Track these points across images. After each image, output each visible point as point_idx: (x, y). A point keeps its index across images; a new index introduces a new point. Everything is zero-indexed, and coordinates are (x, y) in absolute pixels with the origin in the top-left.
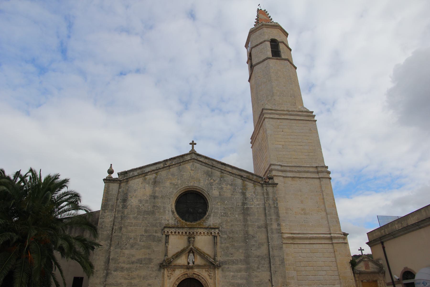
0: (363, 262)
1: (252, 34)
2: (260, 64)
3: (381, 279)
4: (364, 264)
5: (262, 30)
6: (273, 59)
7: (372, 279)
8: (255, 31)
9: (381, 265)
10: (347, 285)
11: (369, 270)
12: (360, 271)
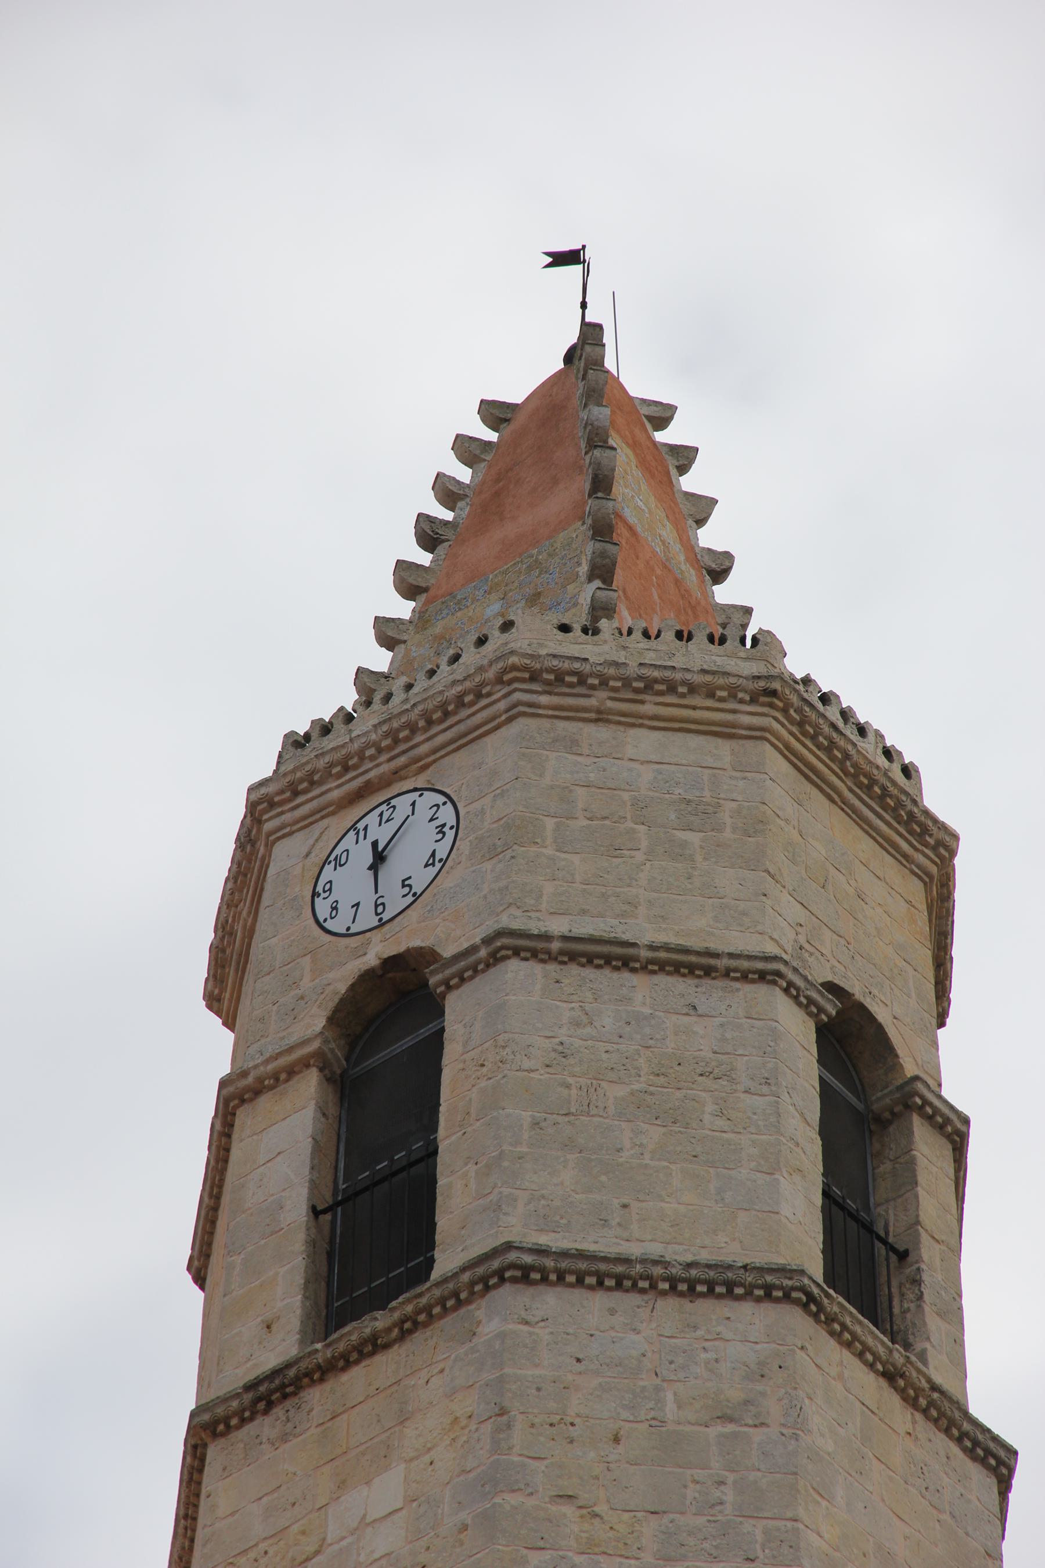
1: (532, 710)
2: (635, 1299)
5: (723, 751)
6: (849, 1345)
8: (599, 699)
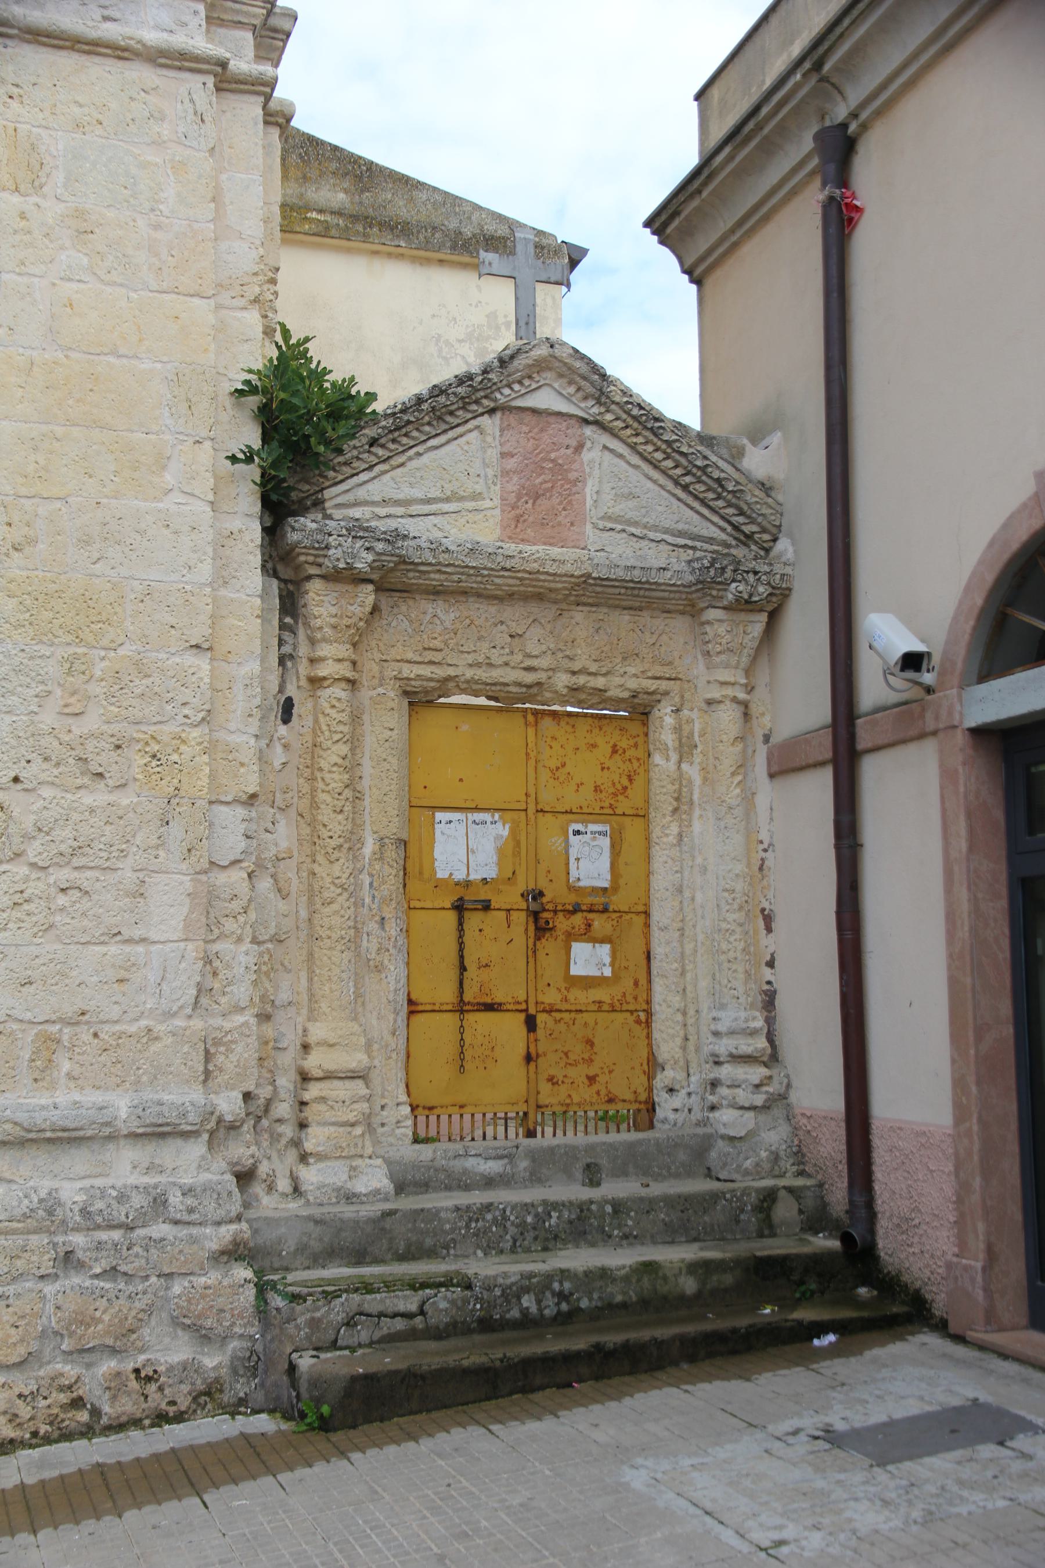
0: (485, 421)
3: (716, 693)
4: (511, 463)
7: (582, 680)
9: (753, 496)
10: (91, 722)
11: (555, 551)
12: (398, 536)
